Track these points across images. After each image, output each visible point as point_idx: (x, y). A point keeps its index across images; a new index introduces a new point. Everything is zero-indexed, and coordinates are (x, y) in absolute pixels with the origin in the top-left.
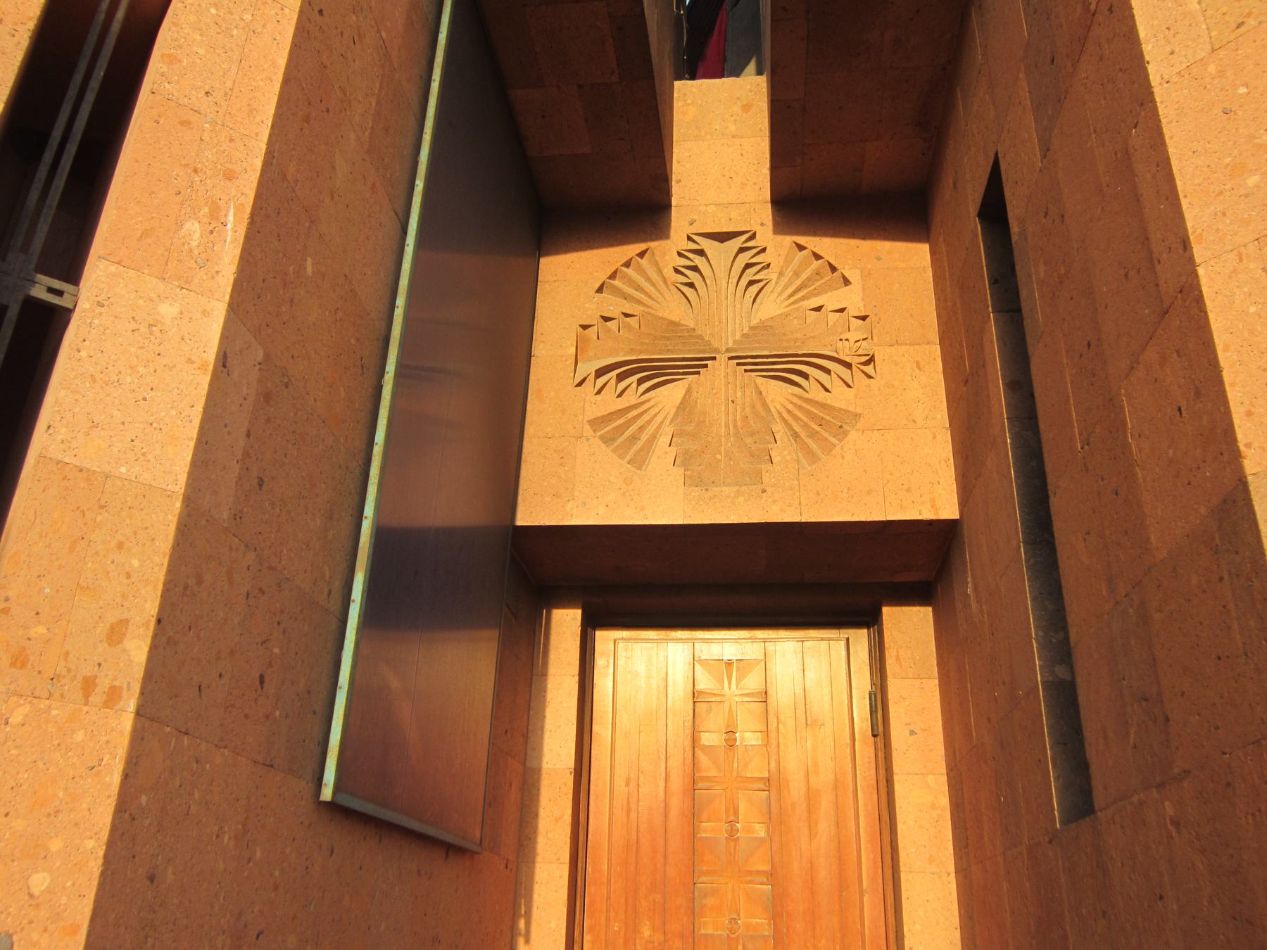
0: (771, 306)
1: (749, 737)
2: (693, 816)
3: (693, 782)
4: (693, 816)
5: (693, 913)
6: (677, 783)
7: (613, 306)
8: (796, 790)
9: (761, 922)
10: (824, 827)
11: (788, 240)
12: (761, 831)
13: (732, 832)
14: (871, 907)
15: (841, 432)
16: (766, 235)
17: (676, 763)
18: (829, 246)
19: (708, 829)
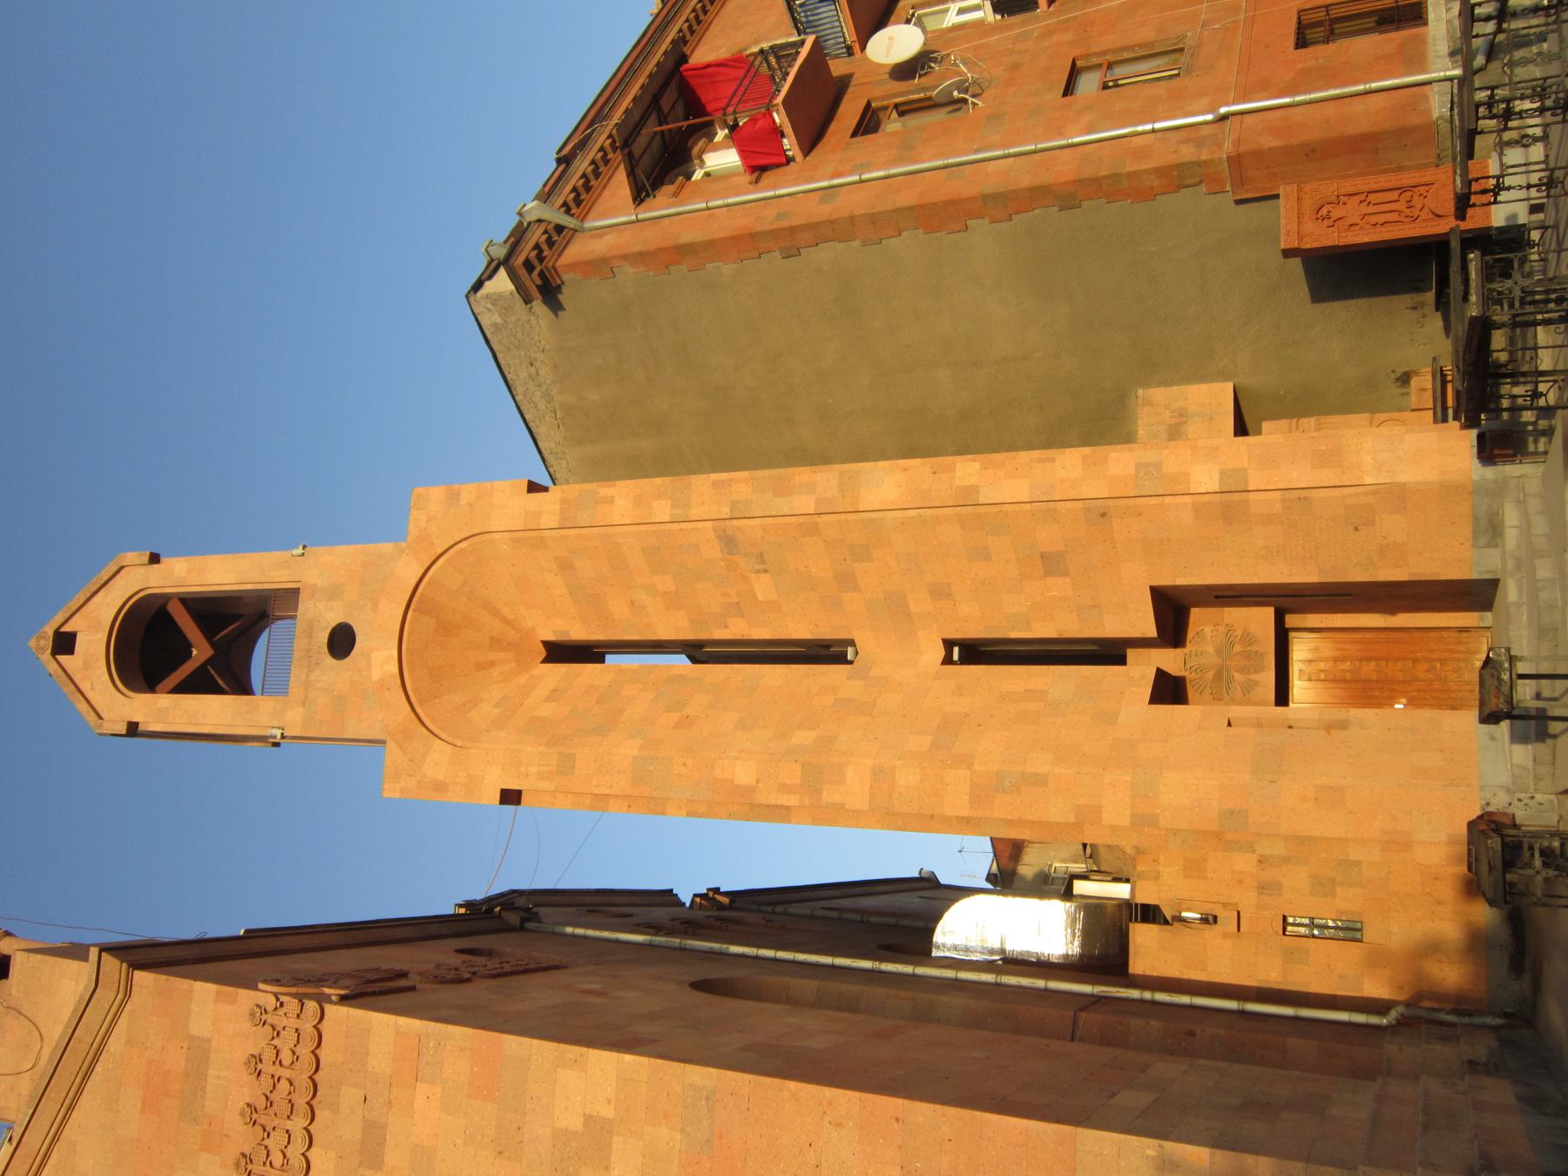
0: (1211, 649)
1: (1322, 665)
2: (1344, 681)
3: (1334, 681)
4: (1344, 681)
5: (1370, 681)
6: (1335, 685)
7: (1208, 691)
8: (1336, 653)
9: (1373, 664)
10: (1346, 646)
11: (1188, 644)
12: (1349, 663)
13: (1348, 671)
14: (1368, 635)
15: (1249, 634)
16: (1186, 650)
17: (1330, 685)
18: (1190, 634)
19: (1348, 676)
